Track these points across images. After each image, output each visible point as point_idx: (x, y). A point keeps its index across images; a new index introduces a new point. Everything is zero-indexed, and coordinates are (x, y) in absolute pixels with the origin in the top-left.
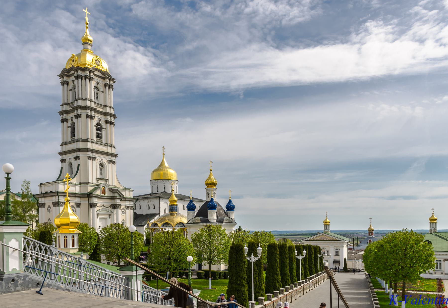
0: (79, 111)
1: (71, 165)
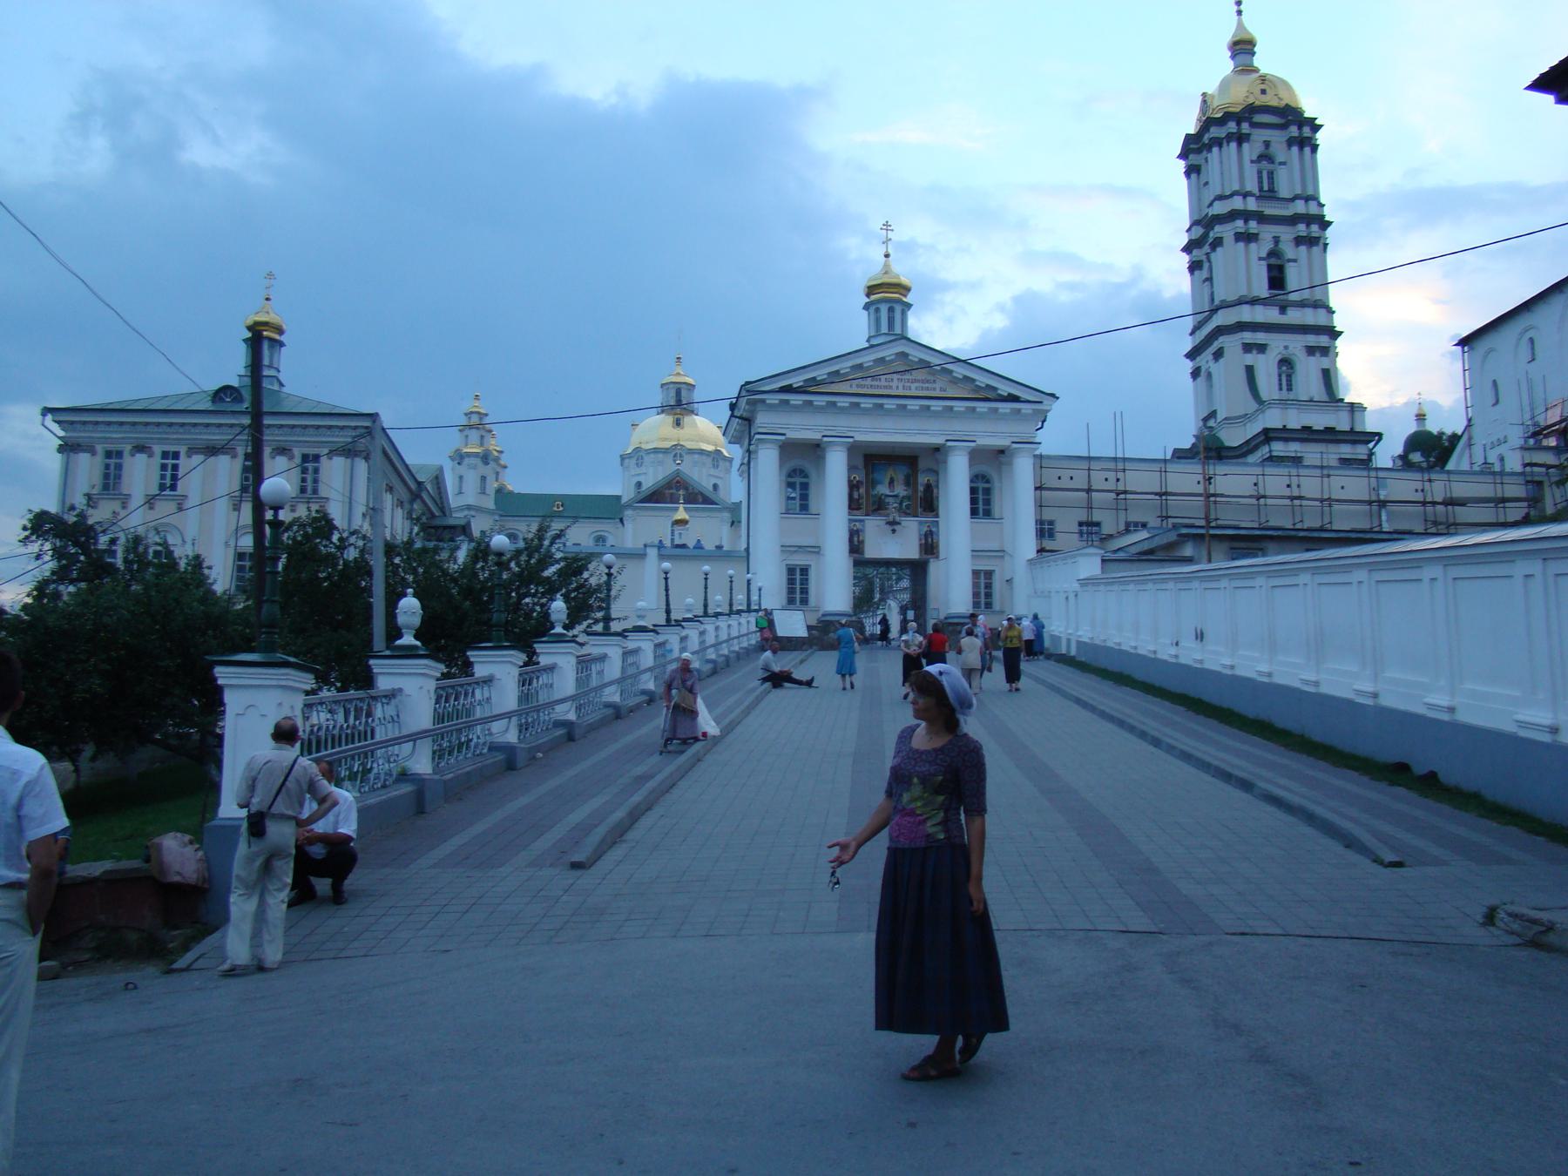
0: (1218, 230)
1: (1209, 375)
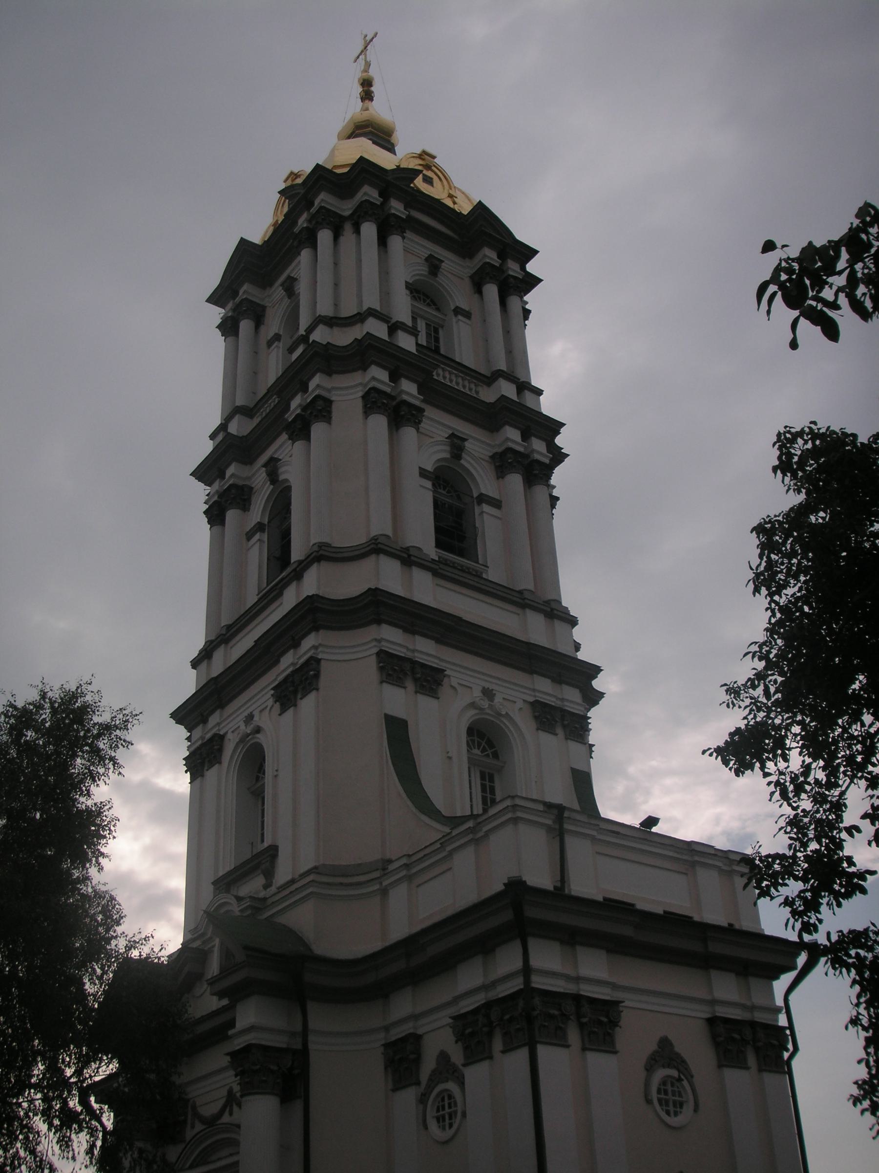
1: (254, 761)
